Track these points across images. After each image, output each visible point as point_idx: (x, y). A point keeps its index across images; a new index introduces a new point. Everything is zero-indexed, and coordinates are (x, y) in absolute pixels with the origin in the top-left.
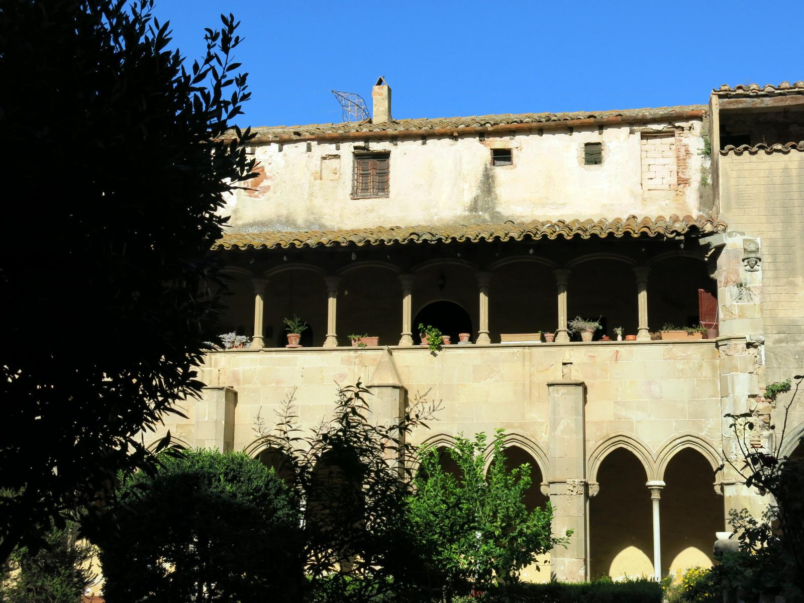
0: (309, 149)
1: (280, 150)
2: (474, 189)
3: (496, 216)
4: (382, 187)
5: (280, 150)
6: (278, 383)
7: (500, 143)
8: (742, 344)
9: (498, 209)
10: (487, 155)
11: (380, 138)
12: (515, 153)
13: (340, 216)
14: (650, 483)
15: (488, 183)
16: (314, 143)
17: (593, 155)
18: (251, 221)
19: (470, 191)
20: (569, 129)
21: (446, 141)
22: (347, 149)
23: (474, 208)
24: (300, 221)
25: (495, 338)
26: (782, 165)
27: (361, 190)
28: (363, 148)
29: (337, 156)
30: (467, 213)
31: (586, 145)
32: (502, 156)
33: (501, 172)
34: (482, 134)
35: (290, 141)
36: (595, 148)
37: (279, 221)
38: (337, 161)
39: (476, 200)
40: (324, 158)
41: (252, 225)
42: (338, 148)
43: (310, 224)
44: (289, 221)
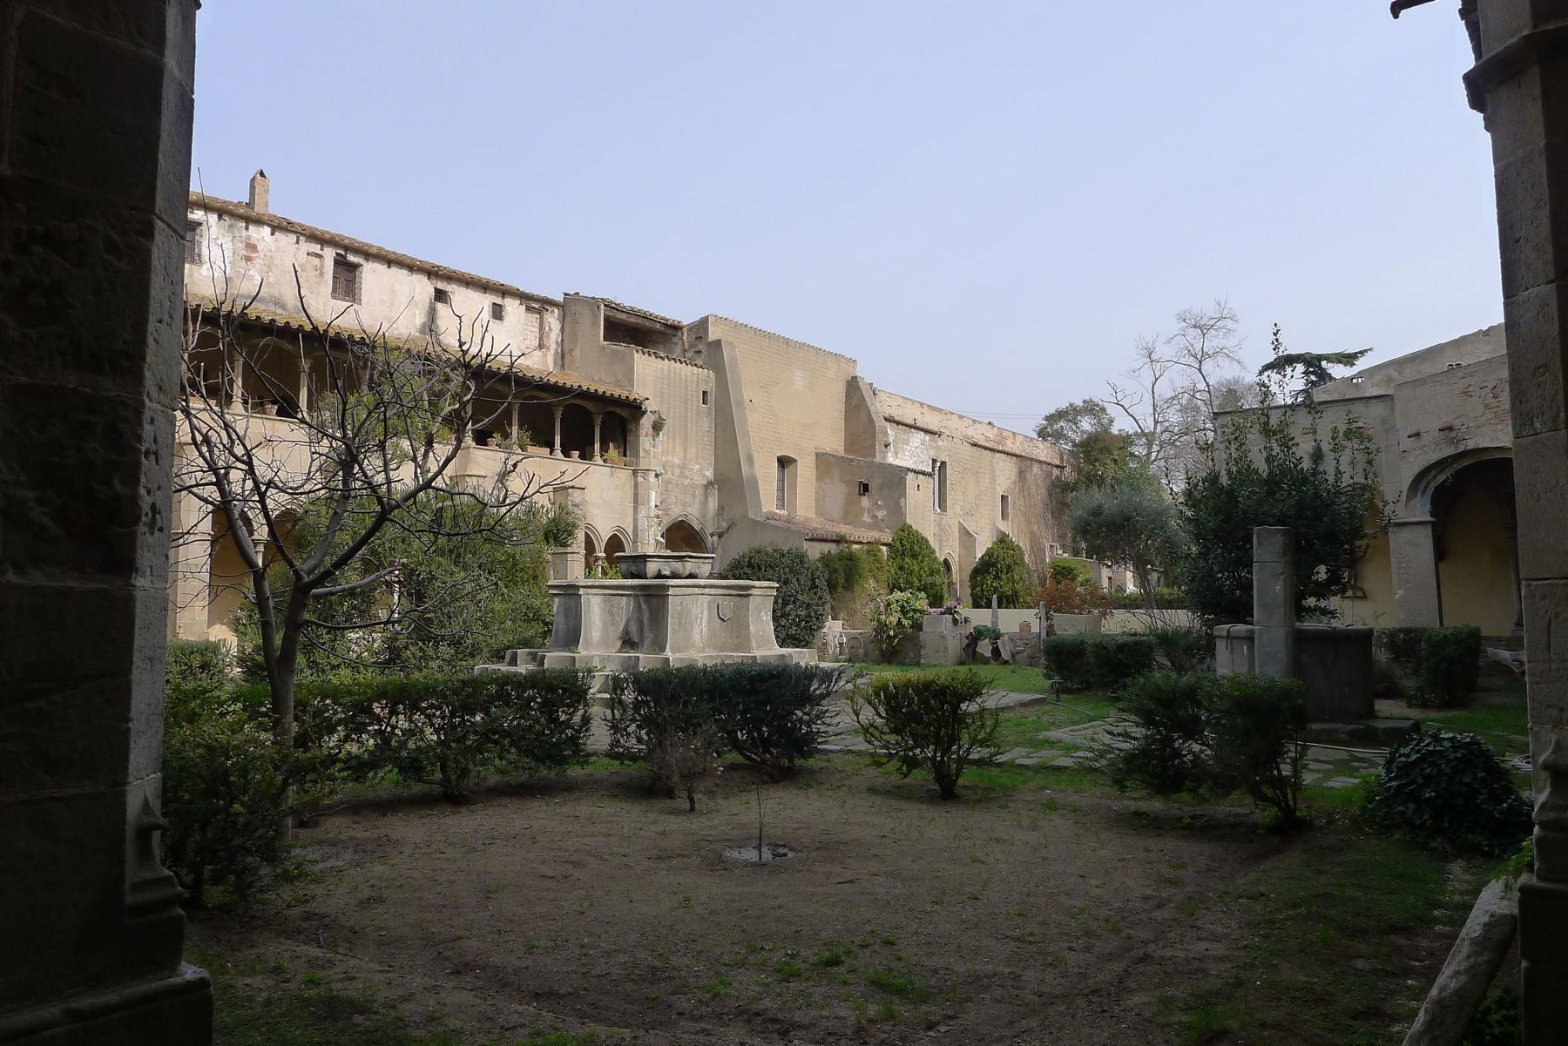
0: (297, 242)
5: (273, 234)
7: (441, 285)
8: (653, 474)
15: (432, 314)
17: (497, 312)
19: (420, 319)
20: (484, 287)
21: (405, 272)
22: (330, 254)
26: (661, 366)
28: (342, 255)
29: (320, 256)
30: (418, 334)
31: (494, 304)
33: (439, 305)
34: (432, 272)
38: (318, 259)
42: (322, 249)
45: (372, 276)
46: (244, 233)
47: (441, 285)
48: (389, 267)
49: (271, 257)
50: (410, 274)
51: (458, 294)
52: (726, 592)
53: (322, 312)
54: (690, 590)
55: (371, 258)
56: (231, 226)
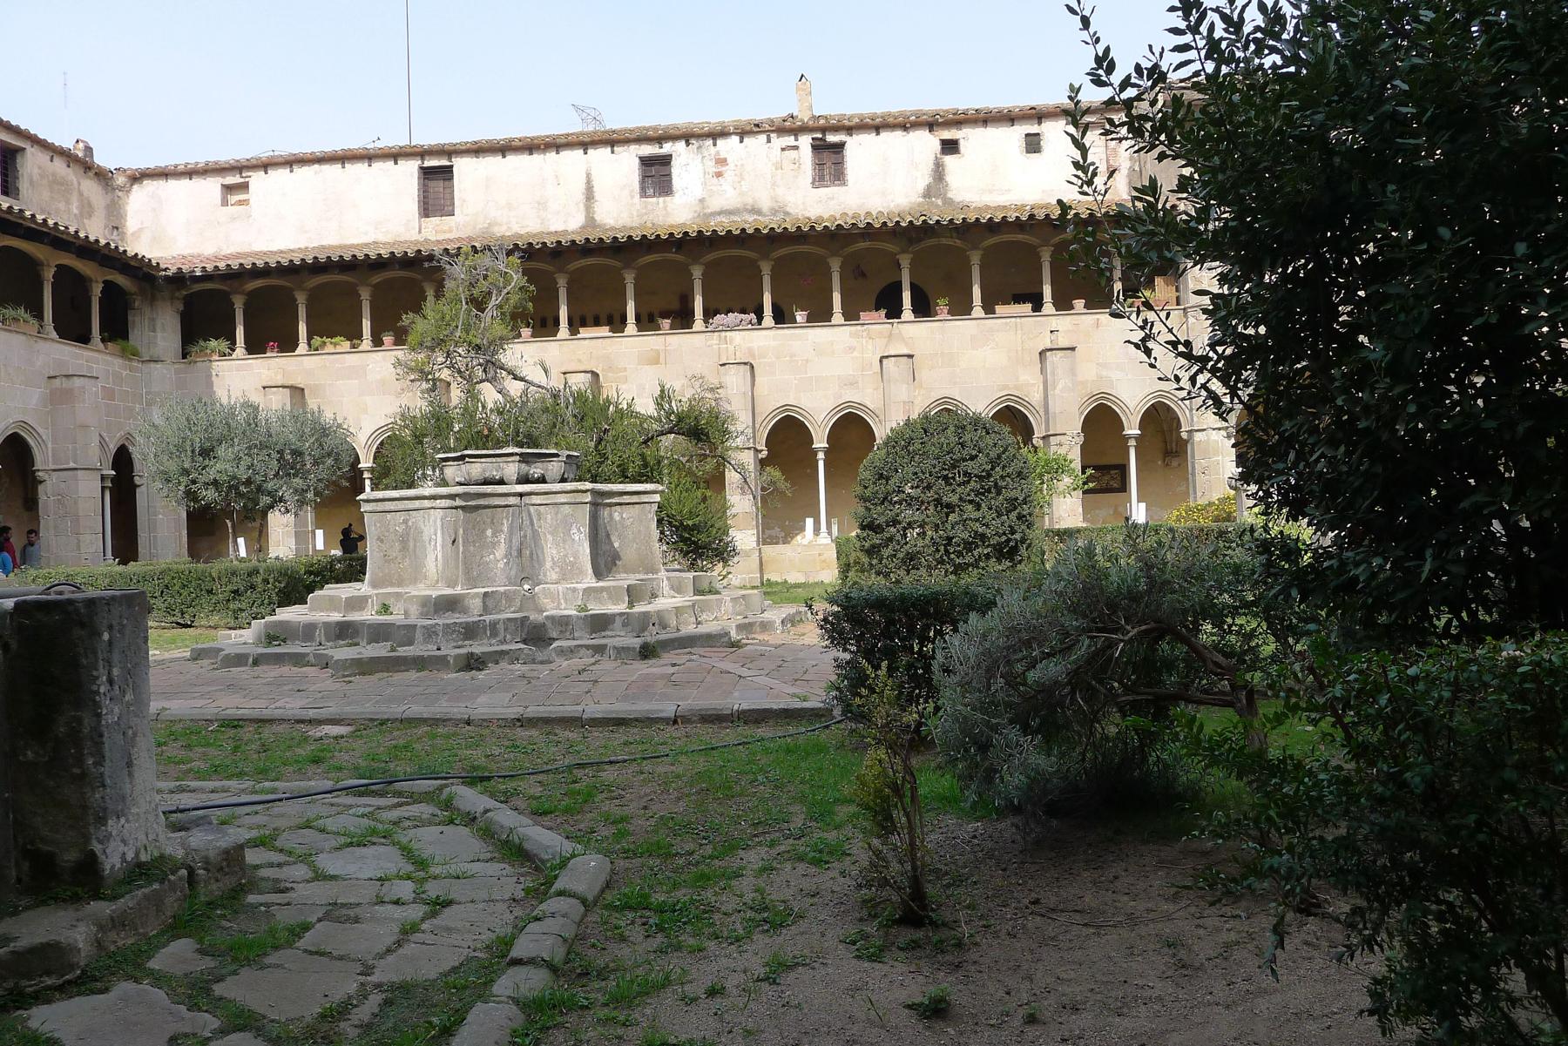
0: (769, 141)
1: (741, 142)
2: (927, 177)
3: (949, 202)
4: (839, 176)
5: (741, 142)
6: (791, 357)
7: (948, 134)
9: (950, 195)
10: (938, 146)
11: (836, 129)
12: (962, 144)
13: (803, 203)
14: (1127, 432)
15: (939, 172)
16: (773, 135)
17: (1033, 144)
18: (718, 210)
19: (923, 179)
20: (1009, 118)
21: (899, 133)
22: (805, 141)
23: (928, 193)
24: (765, 209)
25: (989, 308)
27: (819, 180)
29: (796, 148)
31: (1027, 135)
32: (950, 147)
33: (950, 160)
34: (932, 125)
35: (750, 133)
36: (1035, 138)
37: (746, 210)
39: (929, 187)
40: (783, 149)
41: (720, 213)
42: (796, 140)
43: (775, 212)
44: (756, 211)
45: (858, 148)
46: (713, 150)
47: (948, 134)
48: (878, 134)
49: (742, 165)
50: (905, 133)
51: (964, 135)
52: (459, 502)
53: (801, 207)
54: (417, 504)
55: (854, 131)
56: (699, 147)
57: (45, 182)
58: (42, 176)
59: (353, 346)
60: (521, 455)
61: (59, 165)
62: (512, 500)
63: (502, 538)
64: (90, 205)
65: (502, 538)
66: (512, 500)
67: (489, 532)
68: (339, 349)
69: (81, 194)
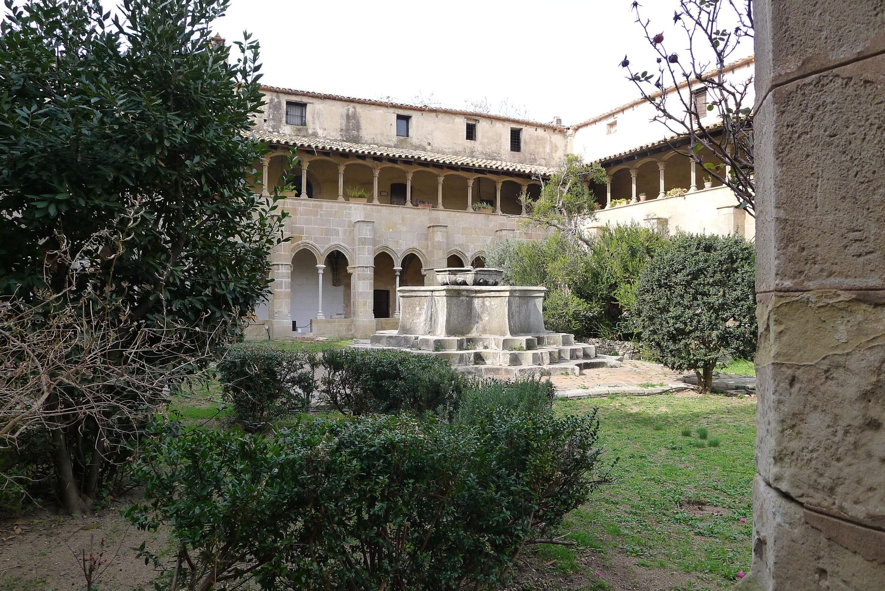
57: (532, 141)
58: (530, 139)
59: (628, 203)
60: (449, 271)
61: (540, 131)
62: (428, 294)
63: (424, 311)
64: (556, 146)
65: (424, 311)
66: (428, 294)
67: (418, 309)
68: (622, 205)
69: (551, 142)
